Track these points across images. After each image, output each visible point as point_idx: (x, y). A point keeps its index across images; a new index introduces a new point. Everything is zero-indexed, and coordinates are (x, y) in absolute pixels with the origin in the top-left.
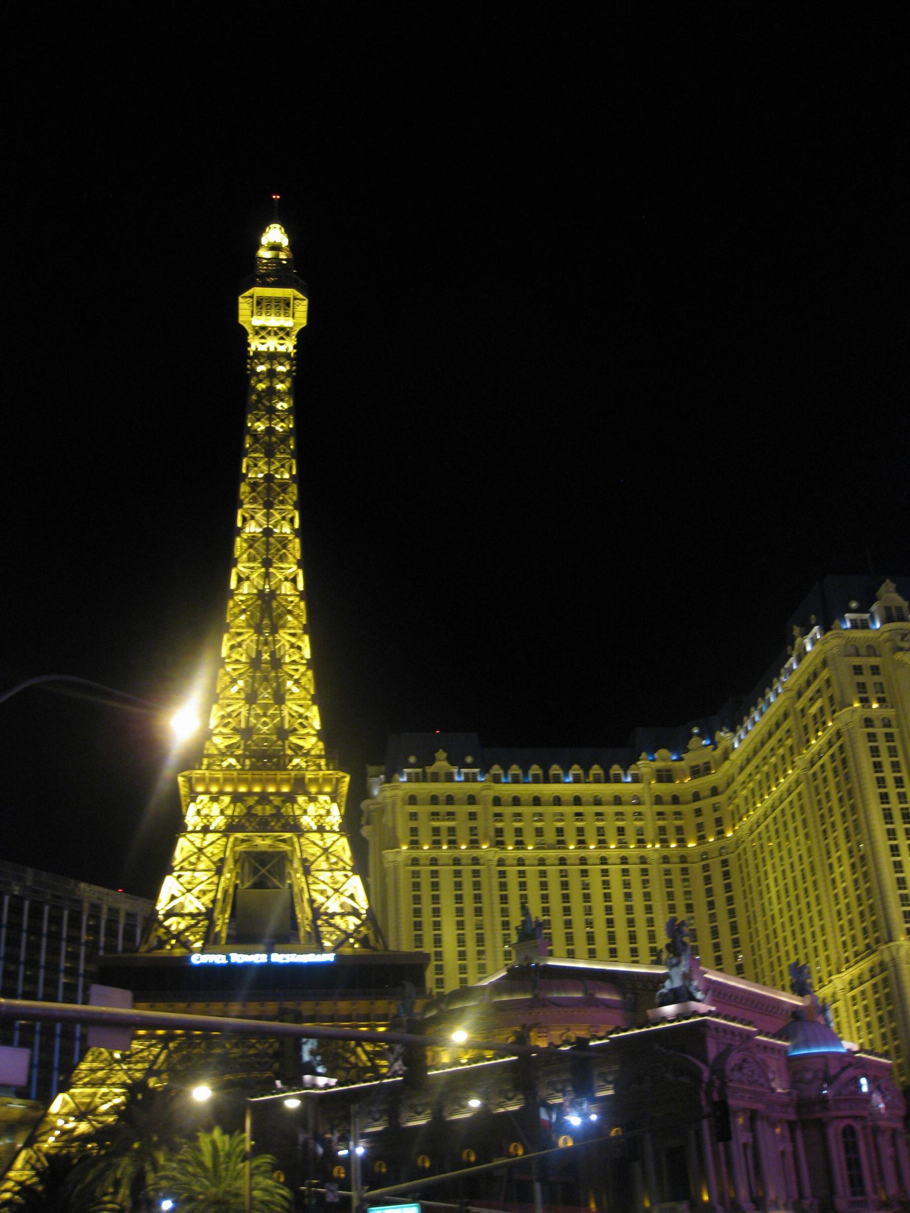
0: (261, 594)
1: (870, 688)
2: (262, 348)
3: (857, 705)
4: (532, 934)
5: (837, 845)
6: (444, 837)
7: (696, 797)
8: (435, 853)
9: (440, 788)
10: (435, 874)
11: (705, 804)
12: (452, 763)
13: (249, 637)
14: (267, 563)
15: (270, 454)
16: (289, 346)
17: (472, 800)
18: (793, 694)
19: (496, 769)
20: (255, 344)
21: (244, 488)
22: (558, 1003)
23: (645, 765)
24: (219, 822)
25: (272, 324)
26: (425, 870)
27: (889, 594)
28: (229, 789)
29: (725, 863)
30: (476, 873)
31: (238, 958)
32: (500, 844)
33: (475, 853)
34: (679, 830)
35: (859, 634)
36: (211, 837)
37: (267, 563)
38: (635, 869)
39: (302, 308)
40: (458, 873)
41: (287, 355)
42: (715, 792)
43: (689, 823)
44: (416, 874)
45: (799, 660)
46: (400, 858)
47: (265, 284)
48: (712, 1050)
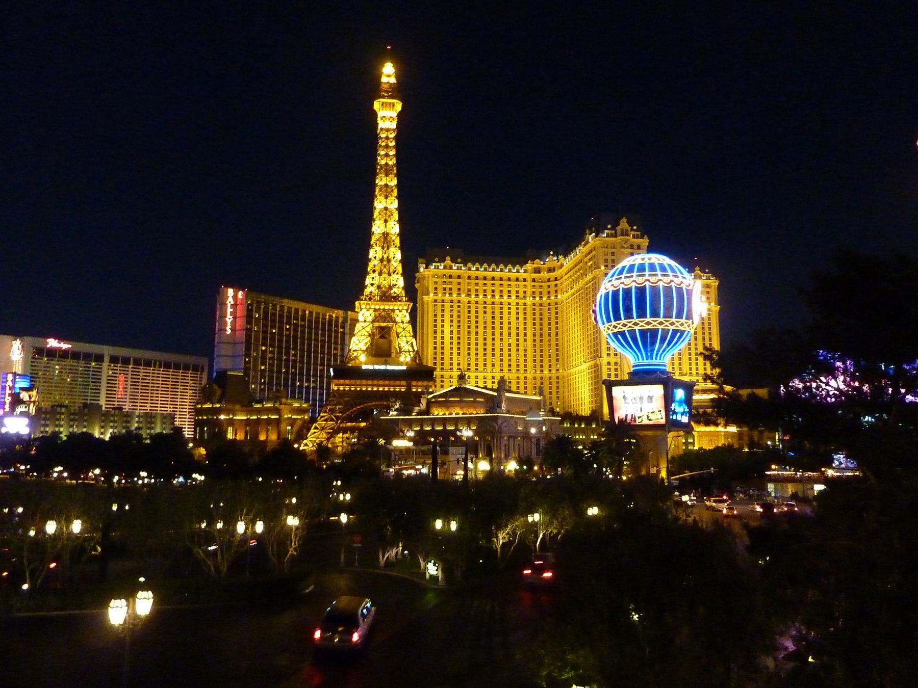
0: (383, 234)
1: (610, 261)
2: (384, 127)
3: (603, 268)
4: (461, 377)
6: (447, 291)
7: (549, 280)
8: (443, 298)
9: (448, 272)
10: (443, 306)
11: (552, 284)
12: (452, 261)
13: (378, 249)
14: (386, 221)
15: (387, 175)
16: (394, 125)
17: (459, 277)
19: (470, 265)
20: (381, 124)
21: (377, 189)
22: (467, 402)
23: (529, 266)
24: (370, 319)
25: (387, 115)
27: (624, 224)
28: (373, 307)
29: (556, 308)
30: (459, 306)
31: (377, 367)
32: (469, 295)
33: (459, 298)
34: (541, 293)
36: (367, 324)
37: (386, 221)
38: (521, 308)
39: (399, 106)
40: (452, 306)
41: (394, 130)
42: (556, 279)
43: (545, 291)
46: (430, 299)
48: (500, 422)
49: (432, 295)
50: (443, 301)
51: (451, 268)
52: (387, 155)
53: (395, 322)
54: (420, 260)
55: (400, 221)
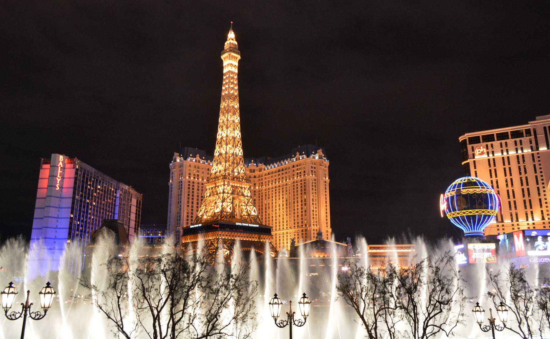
0: (233, 137)
5: (297, 202)
6: (196, 177)
8: (194, 181)
10: (193, 186)
16: (236, 71)
18: (291, 166)
26: (191, 184)
27: (320, 151)
35: (313, 159)
36: (229, 195)
37: (234, 130)
42: (255, 177)
44: (189, 185)
45: (296, 160)
47: (234, 52)
49: (187, 178)
50: (193, 182)
51: (199, 162)
52: (233, 88)
53: (243, 195)
54: (176, 154)
55: (242, 131)
